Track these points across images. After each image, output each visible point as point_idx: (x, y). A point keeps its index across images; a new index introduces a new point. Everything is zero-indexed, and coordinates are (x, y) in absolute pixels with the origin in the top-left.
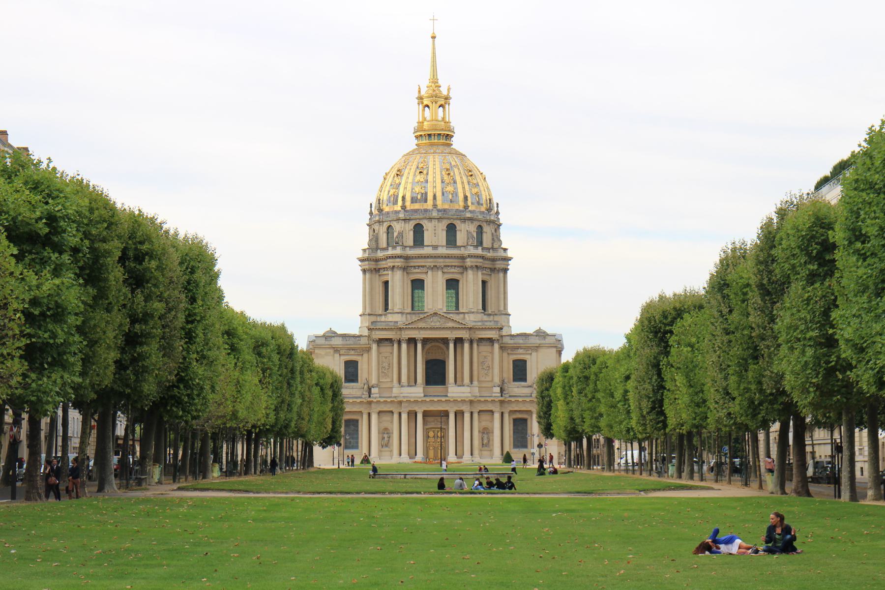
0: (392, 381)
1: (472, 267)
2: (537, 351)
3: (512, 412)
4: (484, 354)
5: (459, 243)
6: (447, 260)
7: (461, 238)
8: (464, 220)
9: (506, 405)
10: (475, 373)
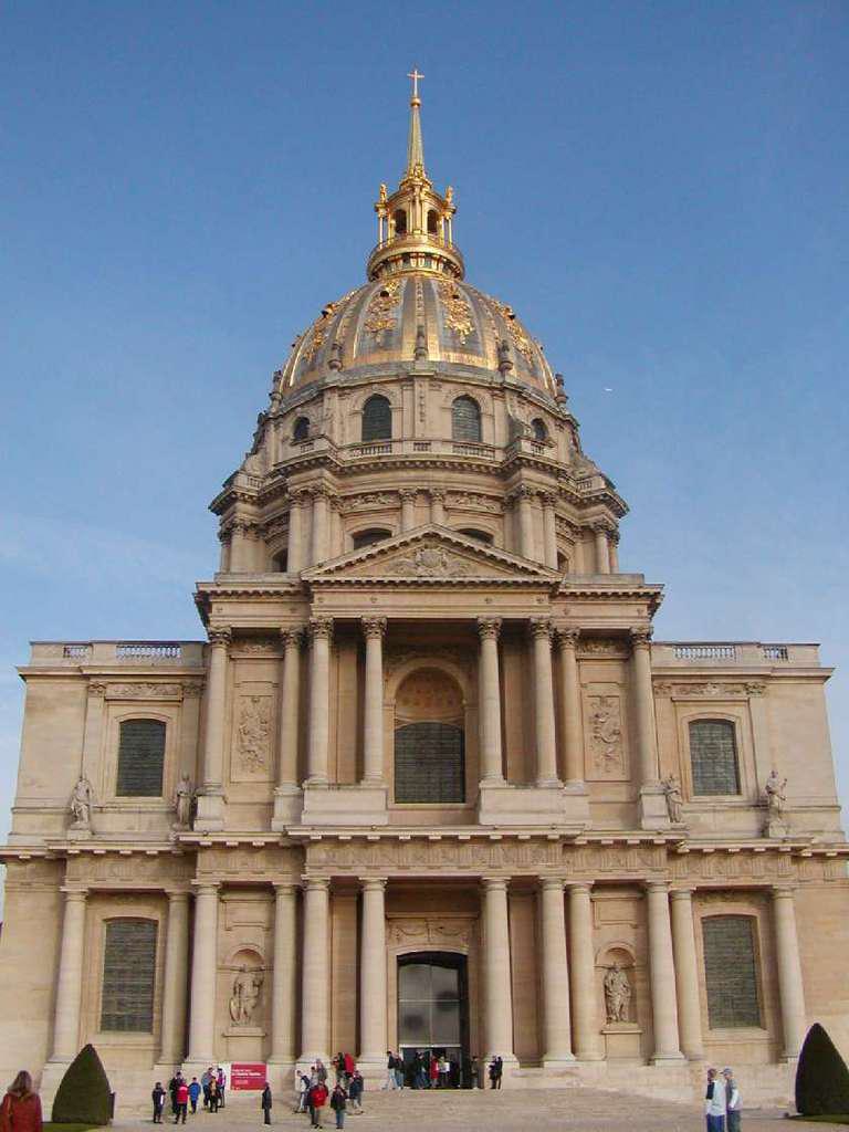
0: (276, 781)
1: (530, 495)
2: (761, 690)
3: (702, 894)
4: (600, 689)
5: (487, 439)
6: (457, 476)
7: (494, 432)
8: (500, 390)
9: (680, 866)
10: (574, 749)
